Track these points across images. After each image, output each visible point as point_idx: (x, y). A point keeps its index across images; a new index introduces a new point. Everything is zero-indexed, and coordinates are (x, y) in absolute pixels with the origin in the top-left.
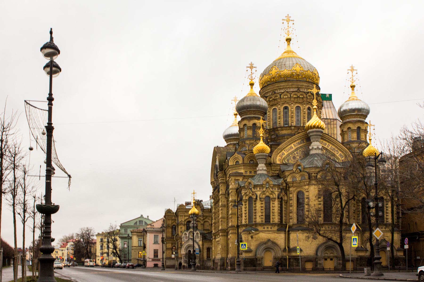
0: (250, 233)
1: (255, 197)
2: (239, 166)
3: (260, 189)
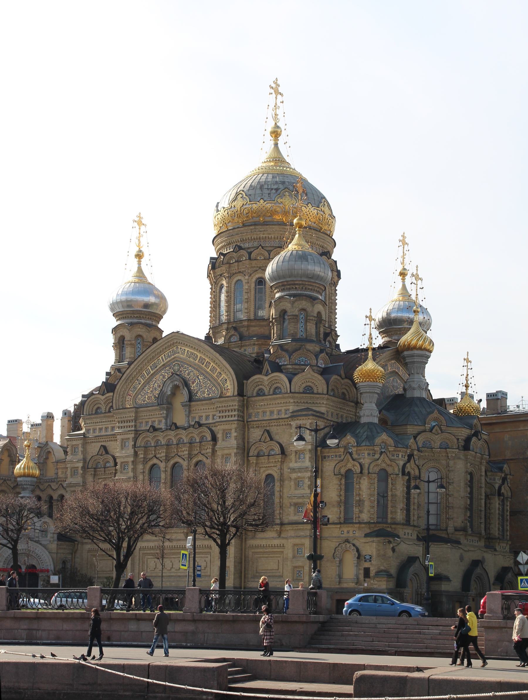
0: (390, 542)
1: (359, 470)
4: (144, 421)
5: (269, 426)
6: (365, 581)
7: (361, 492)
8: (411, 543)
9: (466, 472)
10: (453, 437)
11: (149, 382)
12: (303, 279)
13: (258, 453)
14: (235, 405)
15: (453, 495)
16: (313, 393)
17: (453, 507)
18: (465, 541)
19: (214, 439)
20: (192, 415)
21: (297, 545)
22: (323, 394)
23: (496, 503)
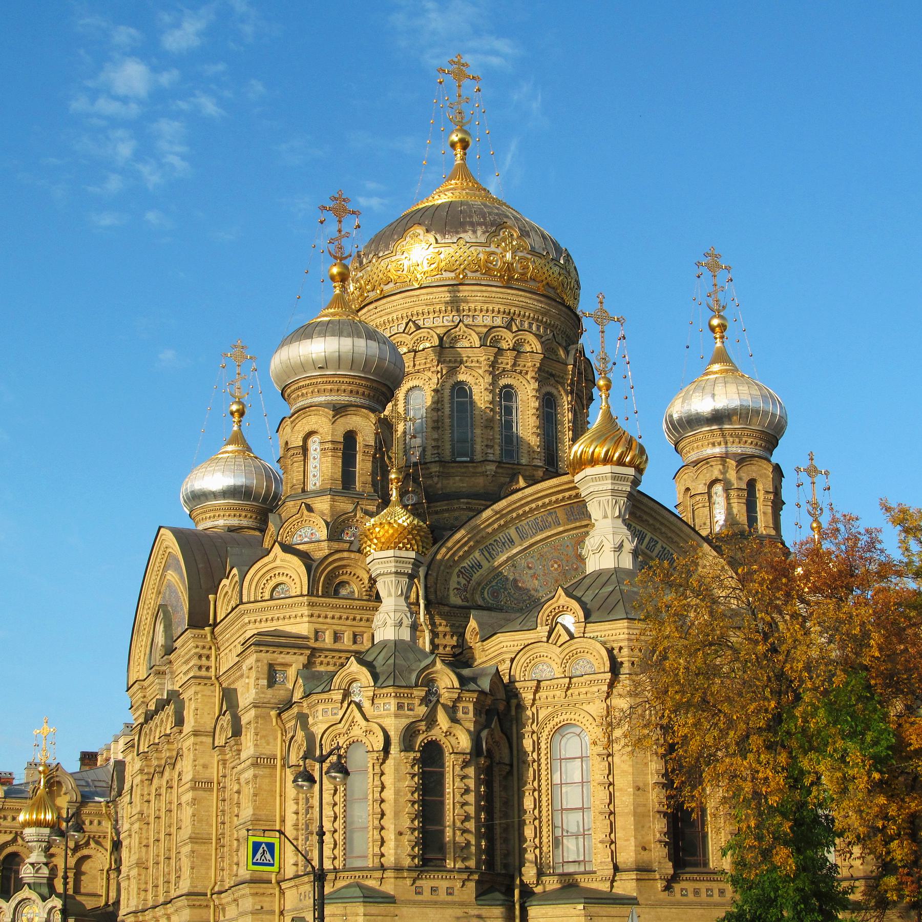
2: (291, 606)
3: (400, 707)
22: (302, 595)
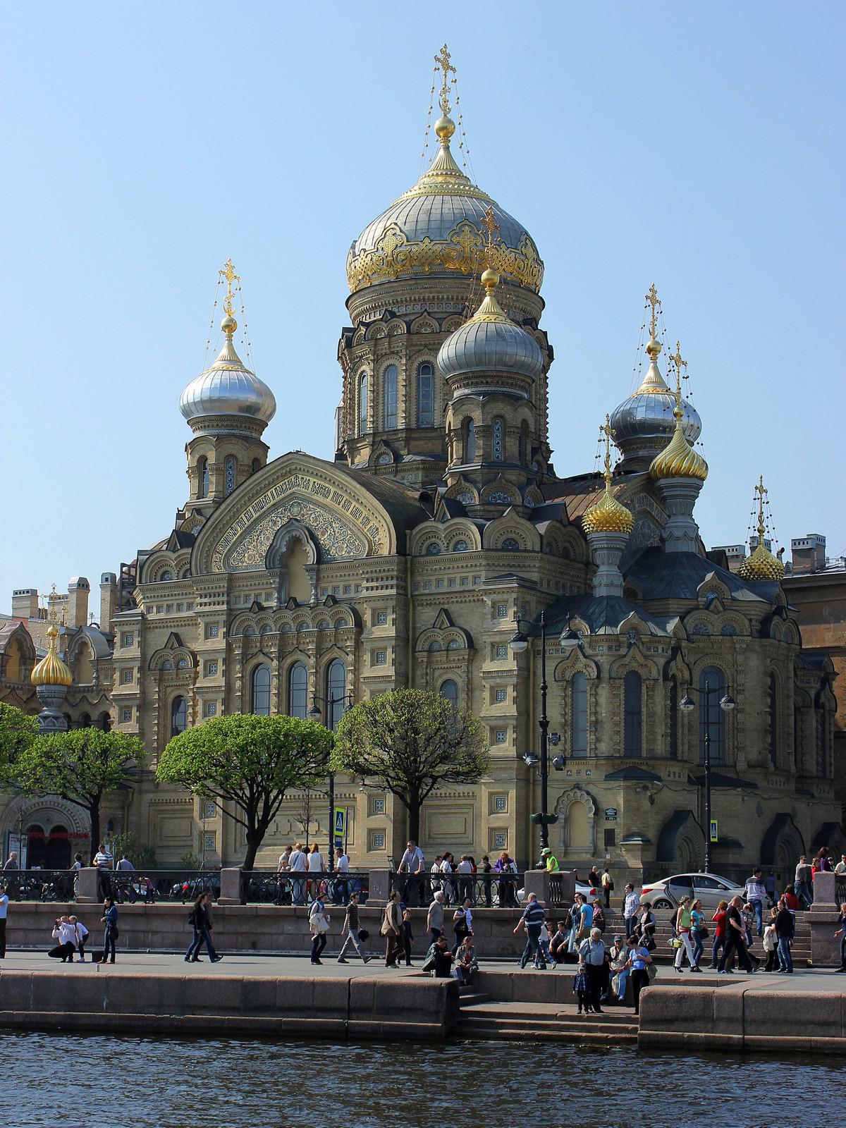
0: (645, 788)
3: (663, 650)
4: (242, 593)
5: (448, 603)
6: (606, 850)
7: (598, 709)
8: (679, 788)
9: (765, 673)
10: (743, 616)
11: (251, 532)
12: (499, 368)
13: (431, 645)
14: (393, 570)
15: (744, 710)
16: (518, 550)
17: (744, 730)
18: (765, 784)
19: (359, 624)
20: (322, 585)
21: (497, 793)
22: (533, 551)
23: (812, 721)
